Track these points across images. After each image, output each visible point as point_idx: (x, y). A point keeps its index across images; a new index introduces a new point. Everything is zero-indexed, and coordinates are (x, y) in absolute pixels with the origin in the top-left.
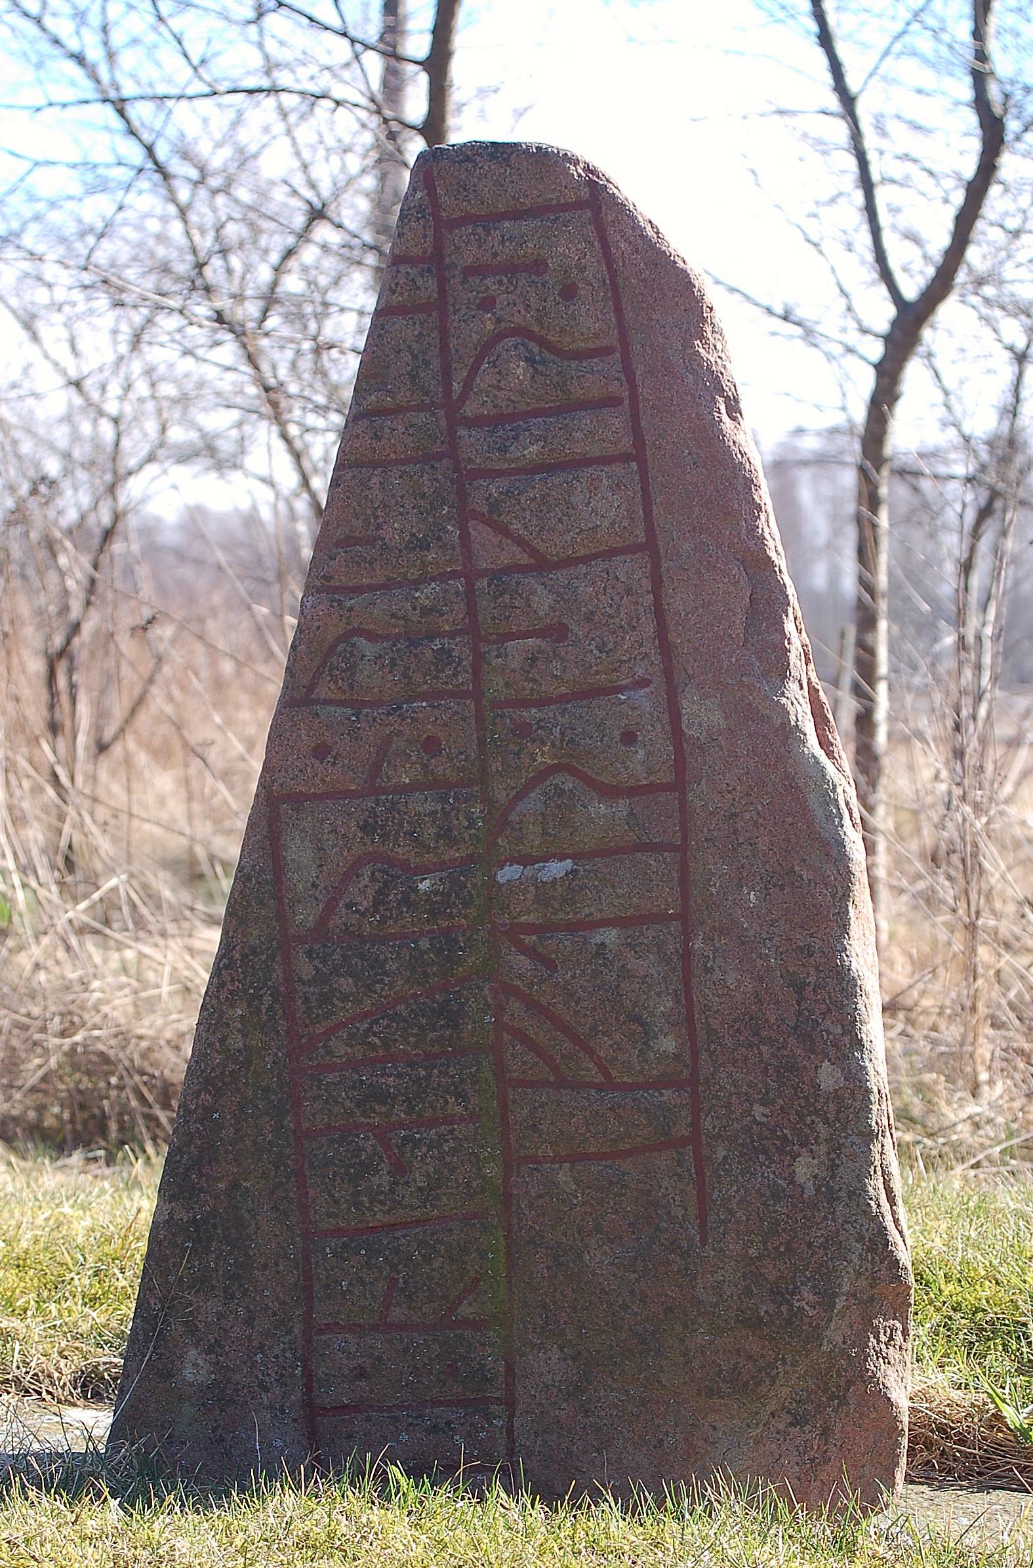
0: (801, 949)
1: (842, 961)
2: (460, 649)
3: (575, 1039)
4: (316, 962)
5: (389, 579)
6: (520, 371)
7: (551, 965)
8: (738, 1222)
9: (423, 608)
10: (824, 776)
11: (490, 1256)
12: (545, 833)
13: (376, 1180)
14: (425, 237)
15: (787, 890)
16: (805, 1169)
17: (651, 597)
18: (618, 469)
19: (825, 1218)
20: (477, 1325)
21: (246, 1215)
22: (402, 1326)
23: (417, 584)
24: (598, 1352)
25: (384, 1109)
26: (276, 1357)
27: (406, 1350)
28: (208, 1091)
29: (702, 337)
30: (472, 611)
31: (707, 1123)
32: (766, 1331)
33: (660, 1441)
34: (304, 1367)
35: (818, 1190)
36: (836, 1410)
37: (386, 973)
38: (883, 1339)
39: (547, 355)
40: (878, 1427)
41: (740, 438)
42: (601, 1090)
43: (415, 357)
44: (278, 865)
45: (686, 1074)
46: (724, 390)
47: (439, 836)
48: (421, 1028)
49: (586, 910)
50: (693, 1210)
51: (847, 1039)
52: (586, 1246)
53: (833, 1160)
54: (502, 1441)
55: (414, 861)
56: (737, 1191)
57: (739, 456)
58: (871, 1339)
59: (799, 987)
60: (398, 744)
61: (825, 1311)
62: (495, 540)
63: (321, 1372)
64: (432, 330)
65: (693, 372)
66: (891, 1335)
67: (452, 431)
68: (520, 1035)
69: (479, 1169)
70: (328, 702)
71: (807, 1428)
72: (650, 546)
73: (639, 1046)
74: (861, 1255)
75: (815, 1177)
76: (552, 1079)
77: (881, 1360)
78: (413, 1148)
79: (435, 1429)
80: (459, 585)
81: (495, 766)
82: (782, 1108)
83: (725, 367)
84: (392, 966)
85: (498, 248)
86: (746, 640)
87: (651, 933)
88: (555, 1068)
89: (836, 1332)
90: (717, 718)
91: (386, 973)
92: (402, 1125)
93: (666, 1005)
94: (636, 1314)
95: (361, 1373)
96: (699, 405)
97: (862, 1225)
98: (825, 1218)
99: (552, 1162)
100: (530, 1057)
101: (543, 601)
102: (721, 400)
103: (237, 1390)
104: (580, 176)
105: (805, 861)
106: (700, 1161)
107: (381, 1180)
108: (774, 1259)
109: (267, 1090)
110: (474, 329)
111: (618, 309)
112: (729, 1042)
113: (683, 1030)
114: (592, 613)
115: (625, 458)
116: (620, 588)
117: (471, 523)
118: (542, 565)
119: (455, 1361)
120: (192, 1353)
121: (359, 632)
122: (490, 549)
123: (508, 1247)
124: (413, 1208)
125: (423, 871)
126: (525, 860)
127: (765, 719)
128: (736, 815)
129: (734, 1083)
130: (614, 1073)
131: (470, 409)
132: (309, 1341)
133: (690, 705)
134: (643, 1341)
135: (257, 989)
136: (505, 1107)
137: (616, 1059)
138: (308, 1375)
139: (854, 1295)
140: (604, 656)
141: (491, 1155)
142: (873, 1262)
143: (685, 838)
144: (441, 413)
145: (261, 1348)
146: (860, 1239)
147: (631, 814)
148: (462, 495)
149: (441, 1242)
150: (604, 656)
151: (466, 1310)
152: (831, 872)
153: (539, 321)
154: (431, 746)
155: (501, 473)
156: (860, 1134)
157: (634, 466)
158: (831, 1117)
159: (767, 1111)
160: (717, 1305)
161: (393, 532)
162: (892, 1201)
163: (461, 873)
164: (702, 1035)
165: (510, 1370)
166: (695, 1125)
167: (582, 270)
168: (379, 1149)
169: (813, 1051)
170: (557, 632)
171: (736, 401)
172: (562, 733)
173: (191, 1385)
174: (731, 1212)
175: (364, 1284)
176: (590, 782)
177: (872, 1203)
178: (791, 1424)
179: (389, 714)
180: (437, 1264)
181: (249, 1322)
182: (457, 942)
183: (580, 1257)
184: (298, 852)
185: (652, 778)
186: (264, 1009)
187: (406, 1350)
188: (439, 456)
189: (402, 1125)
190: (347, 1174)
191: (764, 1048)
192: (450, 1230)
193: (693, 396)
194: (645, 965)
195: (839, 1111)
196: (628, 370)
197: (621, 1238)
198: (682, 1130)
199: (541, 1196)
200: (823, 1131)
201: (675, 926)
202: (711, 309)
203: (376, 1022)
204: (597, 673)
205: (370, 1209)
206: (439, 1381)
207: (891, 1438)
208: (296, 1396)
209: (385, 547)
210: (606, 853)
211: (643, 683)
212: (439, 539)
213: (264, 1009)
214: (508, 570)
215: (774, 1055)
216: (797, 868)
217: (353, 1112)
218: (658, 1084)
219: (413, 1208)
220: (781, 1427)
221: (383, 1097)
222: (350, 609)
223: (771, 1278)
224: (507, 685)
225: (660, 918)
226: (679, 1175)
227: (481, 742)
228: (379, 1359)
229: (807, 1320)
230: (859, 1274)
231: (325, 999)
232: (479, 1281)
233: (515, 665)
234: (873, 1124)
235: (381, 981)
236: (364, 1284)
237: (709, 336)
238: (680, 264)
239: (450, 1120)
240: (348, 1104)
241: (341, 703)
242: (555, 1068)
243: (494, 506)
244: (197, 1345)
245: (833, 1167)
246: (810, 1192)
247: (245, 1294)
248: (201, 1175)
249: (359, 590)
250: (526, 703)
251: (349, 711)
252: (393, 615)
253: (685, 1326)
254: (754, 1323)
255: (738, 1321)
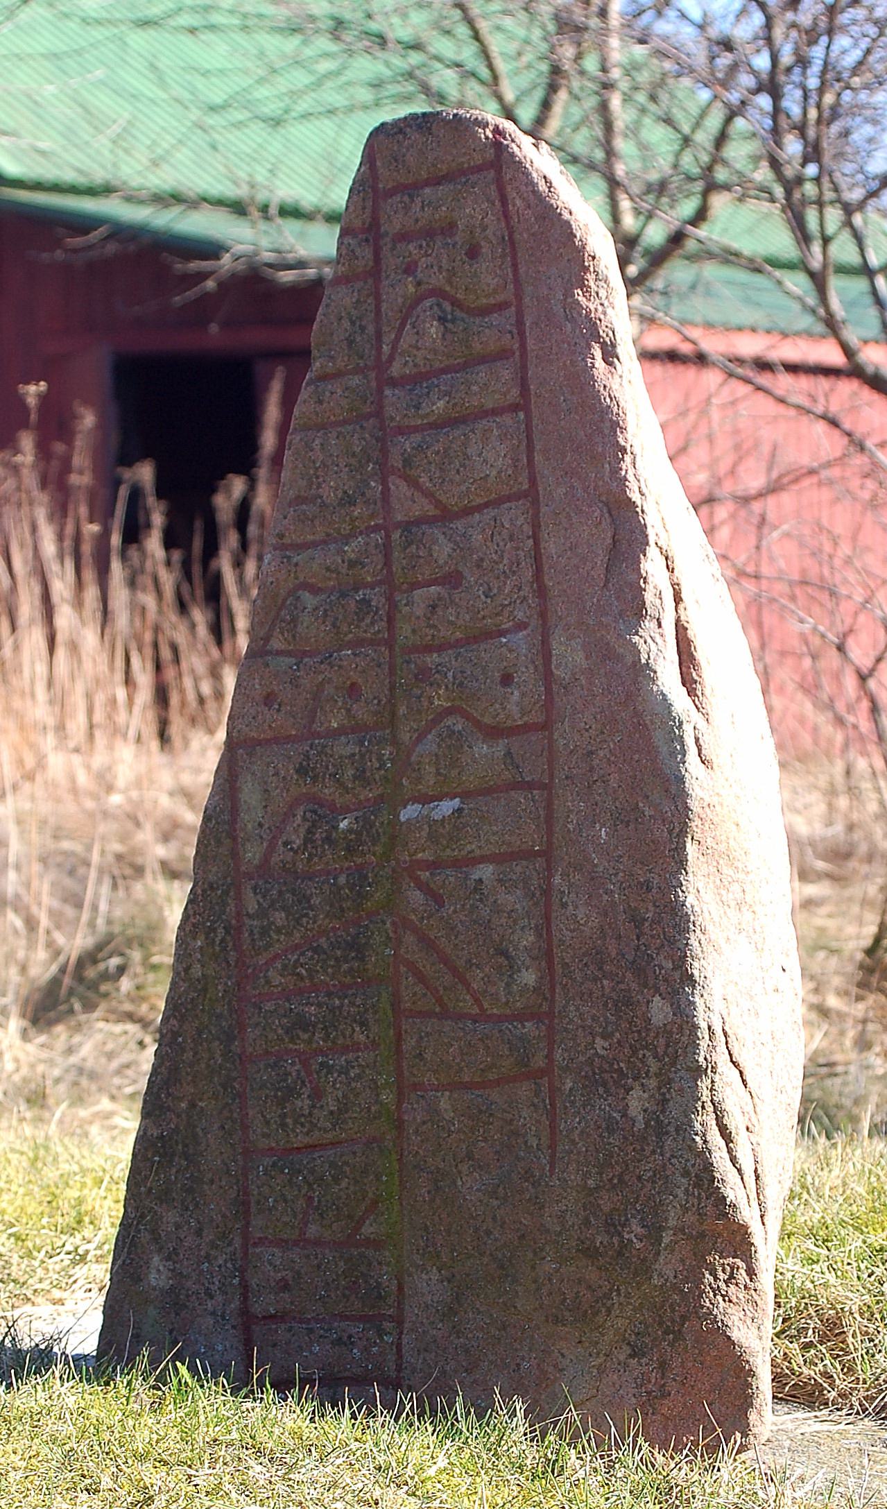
0: (642, 884)
1: (677, 896)
2: (377, 598)
3: (454, 971)
4: (259, 897)
5: (328, 535)
6: (433, 330)
7: (439, 901)
8: (579, 1153)
9: (350, 561)
10: (670, 712)
11: (384, 1178)
12: (439, 774)
13: (299, 1103)
14: (364, 208)
15: (632, 826)
16: (637, 1102)
17: (531, 542)
18: (507, 419)
19: (654, 1152)
20: (376, 1244)
21: (200, 1133)
22: (318, 1243)
23: (347, 539)
24: (468, 1275)
25: (306, 1036)
26: (220, 1266)
27: (319, 1267)
28: (175, 1017)
29: (582, 285)
30: (387, 563)
31: (558, 1055)
32: (602, 1261)
33: (518, 1365)
34: (242, 1279)
35: (647, 1124)
36: (671, 1344)
37: (311, 908)
38: (721, 1276)
39: (458, 313)
40: (721, 1365)
41: (614, 384)
42: (475, 1022)
43: (353, 323)
44: (234, 811)
45: (545, 1008)
46: (600, 337)
47: (355, 778)
48: (337, 959)
49: (469, 848)
50: (545, 1141)
51: (677, 975)
52: (460, 1172)
53: (664, 1094)
54: (391, 1357)
55: (339, 802)
56: (579, 1123)
57: (608, 400)
58: (707, 1276)
59: (637, 921)
60: (329, 690)
61: (652, 1244)
62: (409, 494)
63: (253, 1282)
64: (368, 296)
65: (572, 320)
66: (732, 1273)
67: (380, 391)
68: (411, 965)
69: (378, 1095)
70: (279, 653)
71: (644, 1361)
72: (531, 495)
73: (505, 979)
74: (687, 1190)
75: (645, 1111)
76: (437, 1010)
77: (720, 1298)
78: (328, 1073)
79: (339, 1342)
80: (378, 538)
81: (402, 710)
82: (619, 1042)
83: (605, 313)
84: (316, 901)
85: (419, 215)
86: (607, 581)
87: (519, 869)
88: (439, 1000)
89: (667, 1266)
90: (580, 657)
91: (311, 908)
92: (321, 1052)
93: (528, 939)
94: (496, 1240)
95: (284, 1286)
96: (574, 353)
97: (687, 1160)
98: (654, 1152)
99: (437, 1091)
100: (419, 989)
101: (443, 550)
102: (596, 346)
103: (188, 1296)
104: (487, 138)
105: (648, 797)
106: (553, 1091)
107: (303, 1103)
108: (608, 1190)
109: (219, 1016)
110: (398, 290)
111: (515, 266)
112: (578, 976)
113: (543, 963)
114: (482, 560)
115: (515, 408)
116: (505, 533)
117: (391, 478)
118: (445, 515)
119: (356, 1277)
120: (156, 1259)
121: (305, 586)
122: (407, 503)
123: (400, 1170)
124: (326, 1131)
125: (346, 810)
126: (425, 800)
127: (619, 658)
128: (592, 753)
129: (581, 1016)
130: (486, 1006)
131: (396, 370)
132: (246, 1253)
133: (558, 646)
134: (502, 1267)
135: (213, 922)
136: (399, 1036)
137: (486, 991)
138: (245, 1286)
139: (682, 1230)
140: (489, 601)
141: (387, 1083)
142: (699, 1198)
143: (552, 776)
144: (373, 375)
145: (207, 1257)
146: (686, 1174)
147: (509, 754)
148: (385, 452)
149: (346, 1163)
150: (489, 601)
151: (368, 1230)
152: (667, 807)
153: (450, 282)
154: (353, 690)
155: (416, 429)
156: (689, 1069)
157: (522, 415)
158: (660, 1051)
159: (606, 1045)
160: (560, 1233)
161: (329, 493)
162: (727, 1136)
163: (372, 813)
164: (559, 969)
165: (400, 1288)
166: (549, 1057)
167: (484, 229)
168: (303, 1074)
169: (645, 985)
170: (453, 579)
171: (613, 346)
172: (454, 677)
173: (154, 1289)
174: (573, 1142)
175: (286, 1201)
176: (477, 724)
177: (698, 1139)
178: (631, 1356)
179: (322, 662)
180: (344, 1185)
181: (199, 1233)
182: (366, 877)
183: (454, 1182)
184: (250, 794)
185: (526, 719)
186: (217, 941)
187: (319, 1267)
188: (368, 416)
189: (321, 1052)
190: (276, 1096)
191: (605, 982)
192: (354, 1153)
193: (569, 344)
194: (511, 899)
195: (667, 1046)
196: (520, 323)
197: (488, 1165)
198: (539, 1062)
199: (424, 1123)
200: (654, 1066)
201: (540, 862)
202: (594, 258)
203: (303, 954)
204: (484, 618)
205: (293, 1131)
206: (344, 1295)
207: (738, 1377)
208: (235, 1304)
209: (324, 505)
210: (488, 791)
211: (521, 626)
212: (363, 494)
213: (217, 941)
214: (418, 522)
215: (613, 989)
216: (641, 805)
217: (283, 1040)
218: (521, 1017)
219: (326, 1131)
220: (622, 1358)
221: (303, 1024)
222: (296, 565)
223: (606, 1209)
224: (414, 631)
225: (529, 855)
226: (534, 1105)
227: (392, 688)
228: (298, 1273)
229: (634, 1252)
230: (686, 1210)
231: (264, 932)
232: (377, 1202)
233: (419, 613)
234: (701, 1059)
235: (306, 915)
236: (286, 1201)
237: (592, 284)
238: (566, 216)
239: (356, 1047)
240: (280, 1031)
241: (289, 653)
242: (439, 1000)
243: (407, 462)
244: (160, 1250)
245: (664, 1102)
246: (640, 1125)
247: (197, 1205)
248: (169, 1095)
249: (305, 546)
250: (429, 649)
251: (293, 660)
252: (328, 569)
253: (535, 1253)
254: (589, 1252)
255: (578, 1250)
